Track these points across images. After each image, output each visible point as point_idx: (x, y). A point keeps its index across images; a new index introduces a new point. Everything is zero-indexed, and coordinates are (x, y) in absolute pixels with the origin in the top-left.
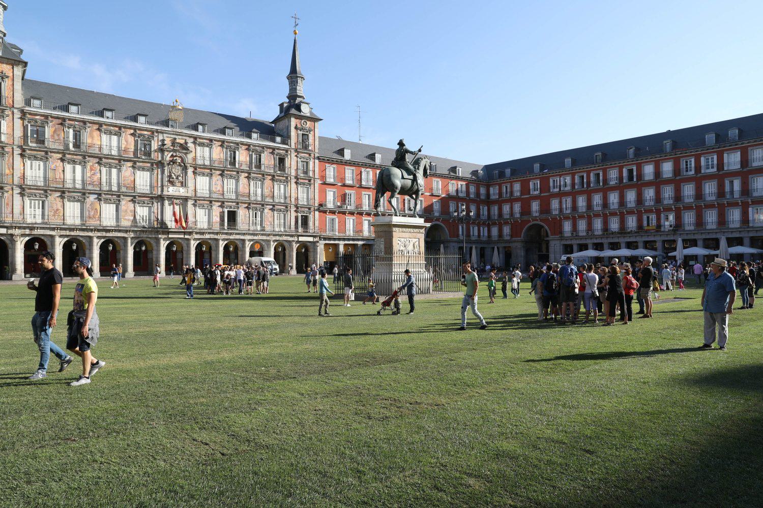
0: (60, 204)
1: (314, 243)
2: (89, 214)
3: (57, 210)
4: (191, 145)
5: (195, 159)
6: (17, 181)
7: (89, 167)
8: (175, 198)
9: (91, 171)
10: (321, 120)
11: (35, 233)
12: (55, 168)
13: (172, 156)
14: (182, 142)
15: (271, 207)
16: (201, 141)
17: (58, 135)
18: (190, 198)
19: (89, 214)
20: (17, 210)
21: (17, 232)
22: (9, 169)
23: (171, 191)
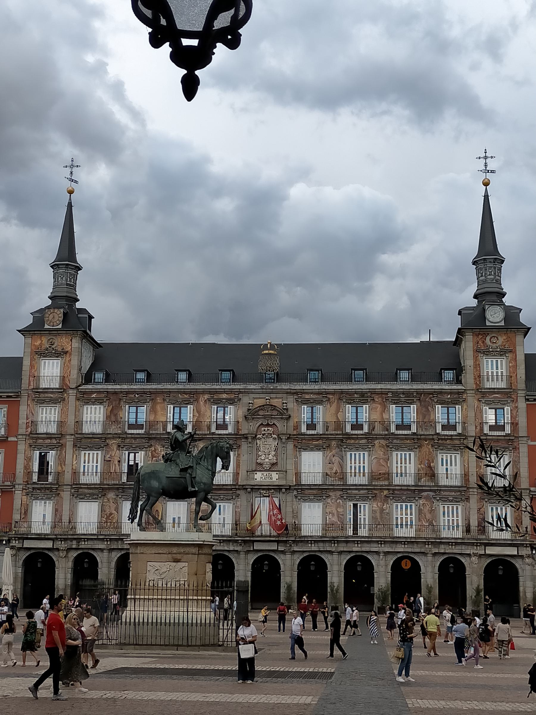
0: (113, 506)
3: (111, 514)
5: (297, 427)
6: (67, 478)
7: (150, 454)
8: (263, 489)
9: (152, 459)
11: (83, 547)
12: (109, 459)
13: (262, 424)
14: (277, 402)
15: (431, 494)
16: (307, 396)
17: (116, 415)
18: (289, 489)
20: (65, 519)
21: (63, 545)
22: (61, 466)
23: (259, 477)
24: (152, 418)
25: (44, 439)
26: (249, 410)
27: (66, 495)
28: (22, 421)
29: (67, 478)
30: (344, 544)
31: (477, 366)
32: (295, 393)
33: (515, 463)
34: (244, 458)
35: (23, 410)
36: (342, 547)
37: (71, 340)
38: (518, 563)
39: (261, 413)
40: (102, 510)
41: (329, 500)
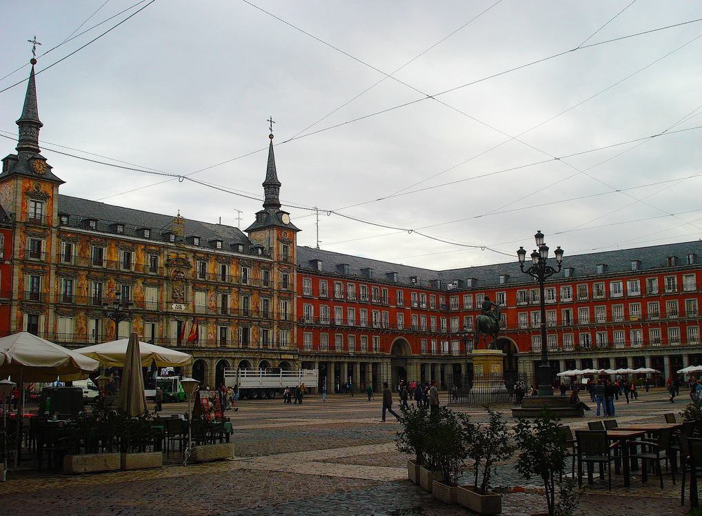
0: (84, 322)
1: (293, 360)
2: (107, 333)
3: (82, 328)
4: (191, 260)
10: (299, 230)
16: (198, 255)
19: (107, 333)
24: (108, 258)
25: (33, 265)
26: (168, 260)
27: (51, 312)
28: (17, 249)
29: (52, 299)
30: (218, 353)
31: (278, 248)
32: (195, 252)
33: (292, 307)
34: (165, 293)
35: (17, 240)
36: (218, 355)
37: (53, 188)
38: (291, 363)
39: (175, 263)
40: (77, 325)
41: (209, 325)
